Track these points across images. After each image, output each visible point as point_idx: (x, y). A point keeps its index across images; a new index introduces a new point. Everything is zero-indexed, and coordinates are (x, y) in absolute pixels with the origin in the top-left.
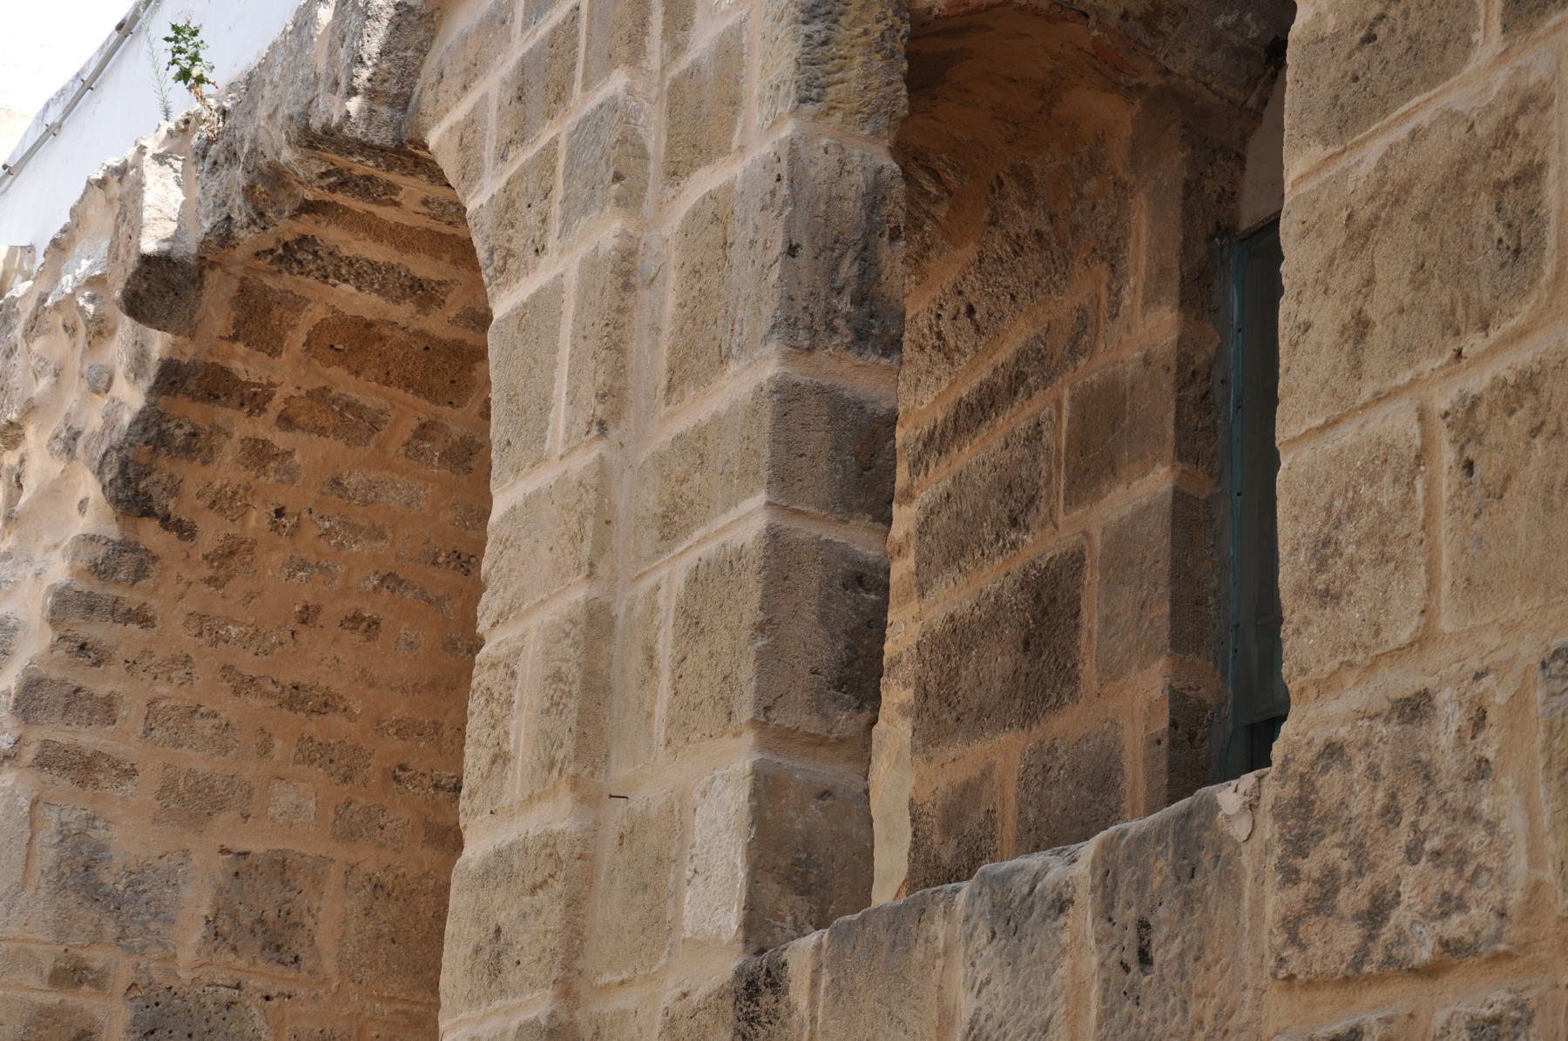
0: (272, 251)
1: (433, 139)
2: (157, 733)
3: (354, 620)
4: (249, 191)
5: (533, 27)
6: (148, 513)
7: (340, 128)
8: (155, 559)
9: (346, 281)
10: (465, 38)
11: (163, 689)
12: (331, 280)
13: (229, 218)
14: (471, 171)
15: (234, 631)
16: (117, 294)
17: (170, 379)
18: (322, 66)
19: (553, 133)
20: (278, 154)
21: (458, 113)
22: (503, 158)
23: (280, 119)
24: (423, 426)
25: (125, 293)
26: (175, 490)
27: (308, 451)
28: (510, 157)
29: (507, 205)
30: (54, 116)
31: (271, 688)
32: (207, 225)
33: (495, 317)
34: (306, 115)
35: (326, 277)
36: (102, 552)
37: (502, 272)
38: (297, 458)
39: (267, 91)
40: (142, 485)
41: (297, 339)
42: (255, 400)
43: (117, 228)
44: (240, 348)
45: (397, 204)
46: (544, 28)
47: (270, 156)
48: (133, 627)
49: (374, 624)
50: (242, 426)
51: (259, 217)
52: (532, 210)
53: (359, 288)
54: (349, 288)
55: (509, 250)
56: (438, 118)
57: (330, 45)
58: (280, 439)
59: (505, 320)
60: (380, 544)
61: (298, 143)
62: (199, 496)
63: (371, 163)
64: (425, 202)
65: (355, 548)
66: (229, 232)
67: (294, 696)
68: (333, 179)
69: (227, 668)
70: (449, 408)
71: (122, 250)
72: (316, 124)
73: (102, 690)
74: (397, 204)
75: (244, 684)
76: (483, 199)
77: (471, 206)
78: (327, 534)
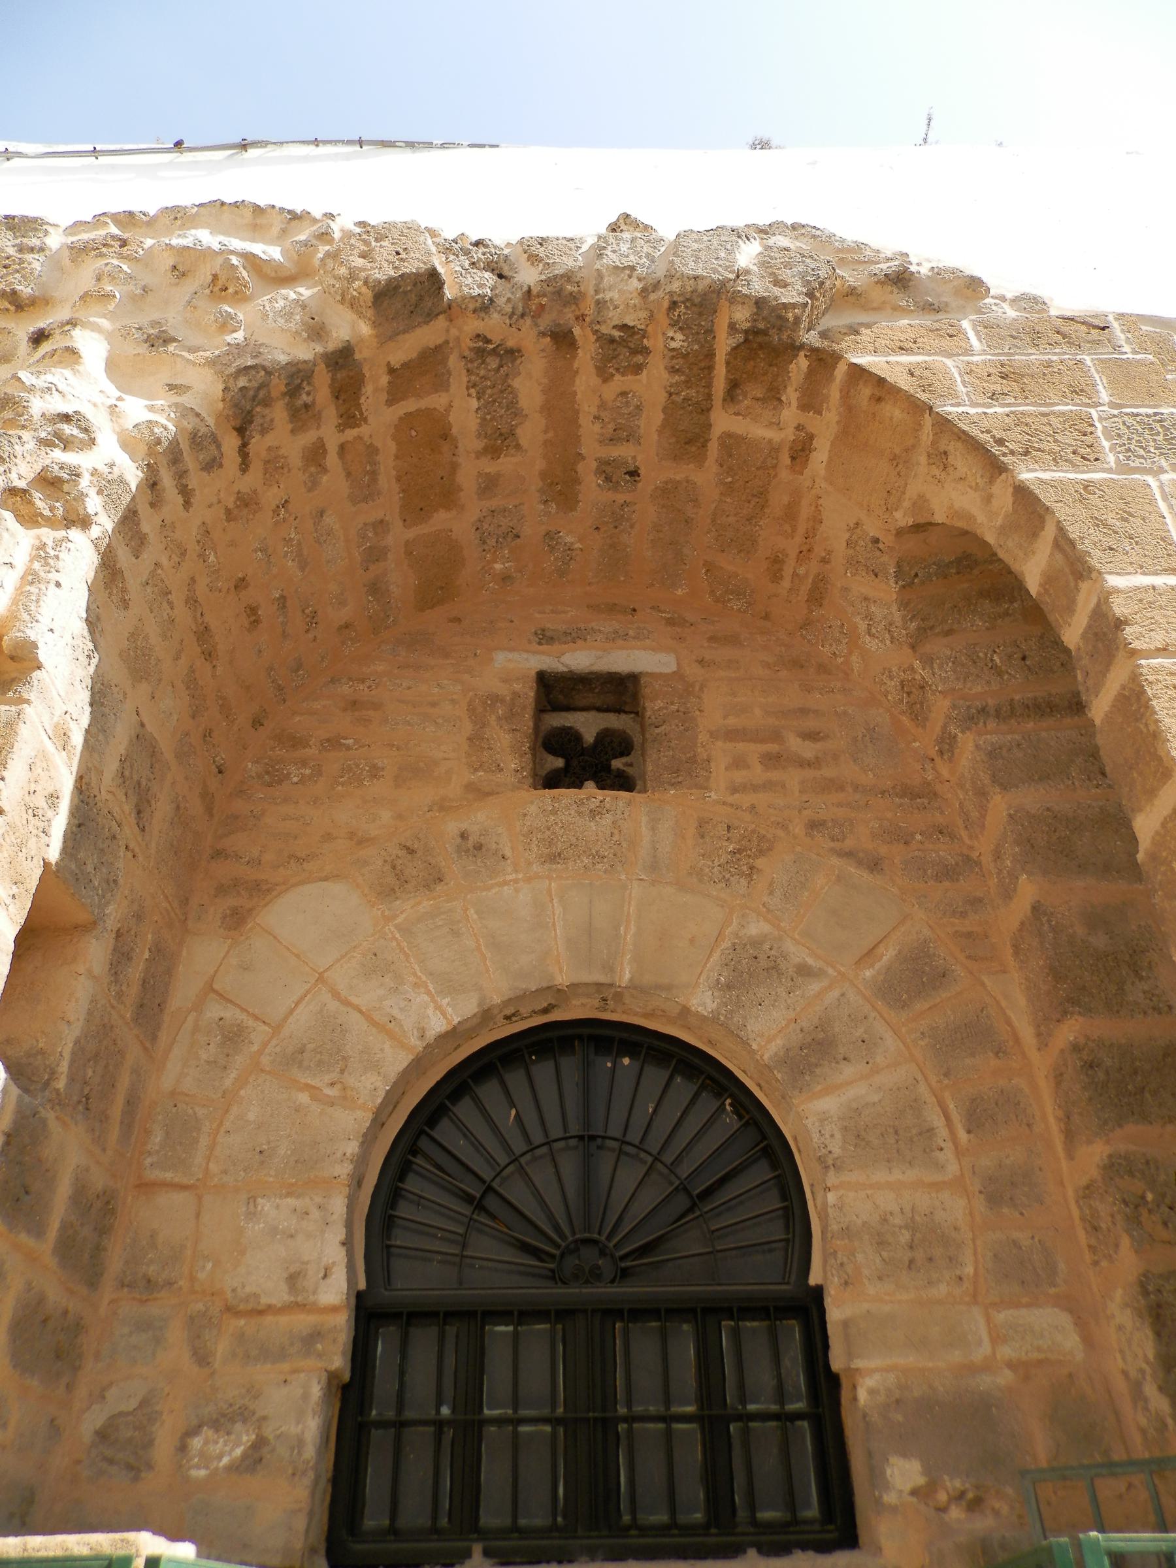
0: (488, 341)
2: (149, 589)
3: (252, 610)
6: (241, 430)
8: (221, 466)
11: (164, 561)
12: (472, 391)
15: (212, 558)
17: (342, 360)
24: (382, 521)
26: (264, 431)
27: (335, 480)
31: (199, 615)
36: (203, 430)
38: (325, 478)
40: (258, 409)
41: (410, 405)
42: (350, 418)
44: (385, 379)
48: (180, 500)
49: (257, 621)
50: (329, 433)
54: (474, 403)
58: (332, 459)
60: (299, 573)
62: (269, 449)
65: (290, 563)
67: (203, 633)
69: (193, 580)
70: (401, 523)
73: (146, 528)
75: (192, 601)
78: (288, 541)
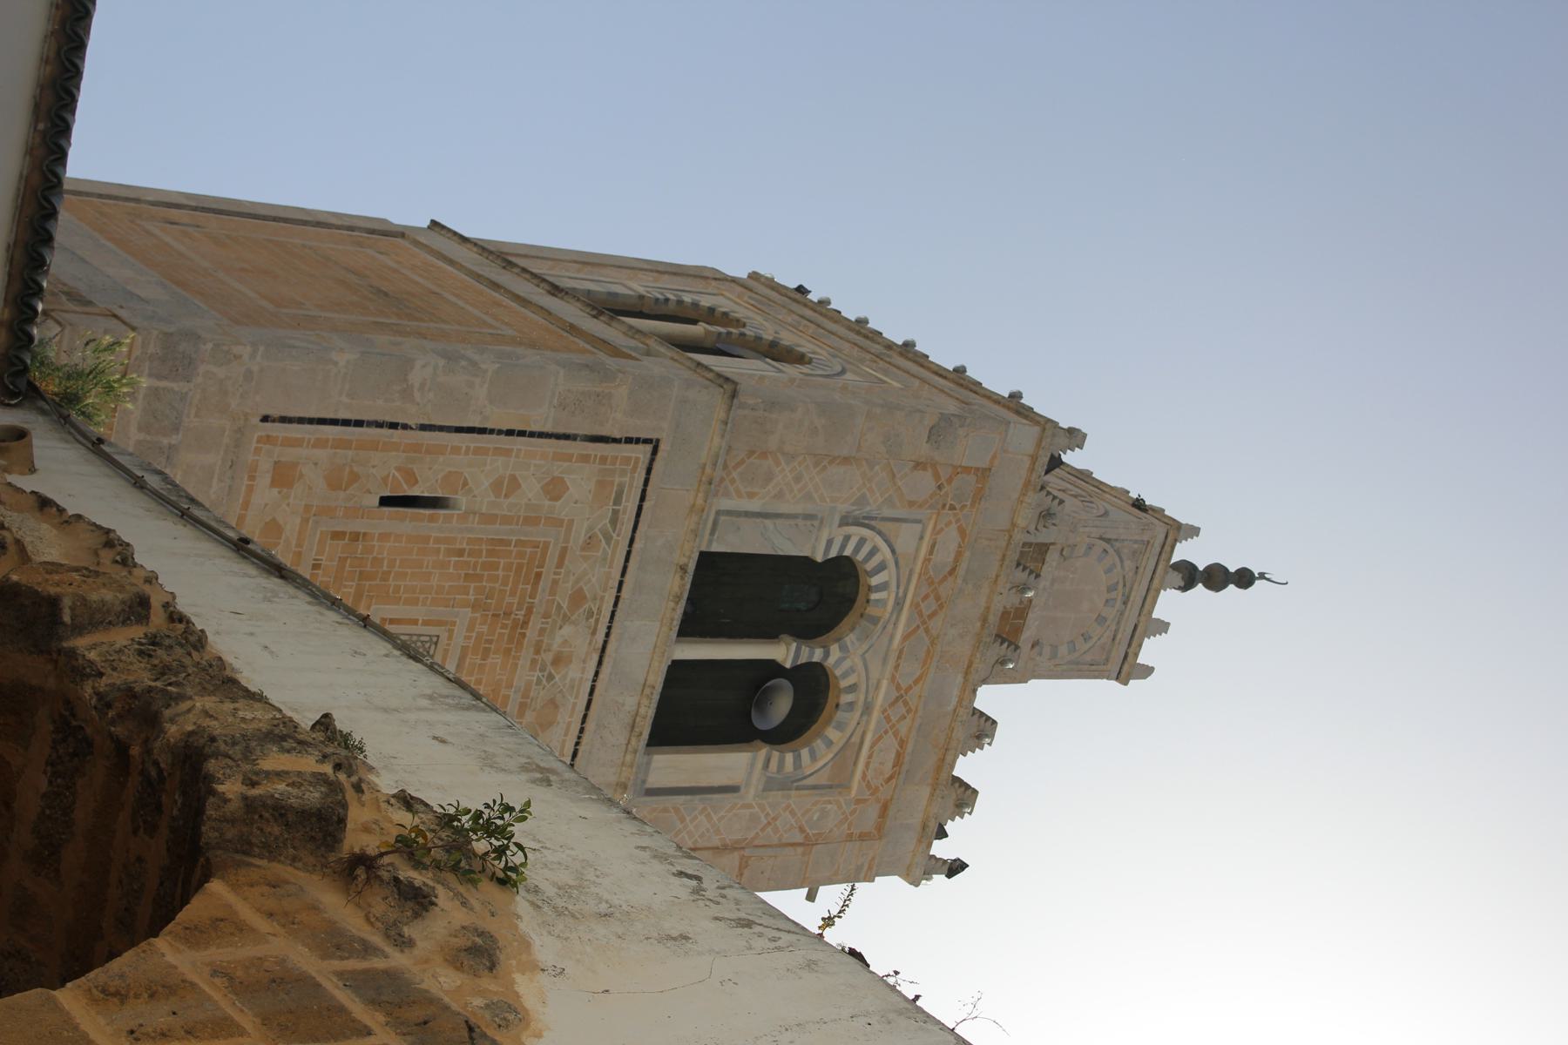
0: (74, 715)
1: (215, 886)
4: (129, 692)
5: (341, 984)
7: (213, 792)
9: (50, 782)
10: (314, 908)
13: (101, 675)
14: (196, 936)
16: (15, 578)
18: (267, 765)
19: (249, 1027)
20: (172, 721)
21: (246, 913)
22: (215, 973)
23: (207, 722)
25: (17, 584)
28: (217, 981)
29: (167, 988)
30: (153, 481)
32: (92, 655)
33: (56, 993)
34: (217, 755)
35: (52, 765)
37: (103, 991)
39: (228, 706)
43: (77, 570)
45: (135, 832)
46: (344, 997)
47: (167, 713)
51: (104, 702)
52: (171, 1018)
53: (44, 795)
54: (44, 786)
55: (126, 996)
56: (235, 887)
57: (287, 773)
59: (57, 1007)
61: (187, 746)
63: (175, 812)
64: (140, 859)
66: (89, 676)
68: (154, 773)
71: (57, 577)
72: (212, 765)
74: (135, 832)
76: (170, 958)
77: (161, 943)
